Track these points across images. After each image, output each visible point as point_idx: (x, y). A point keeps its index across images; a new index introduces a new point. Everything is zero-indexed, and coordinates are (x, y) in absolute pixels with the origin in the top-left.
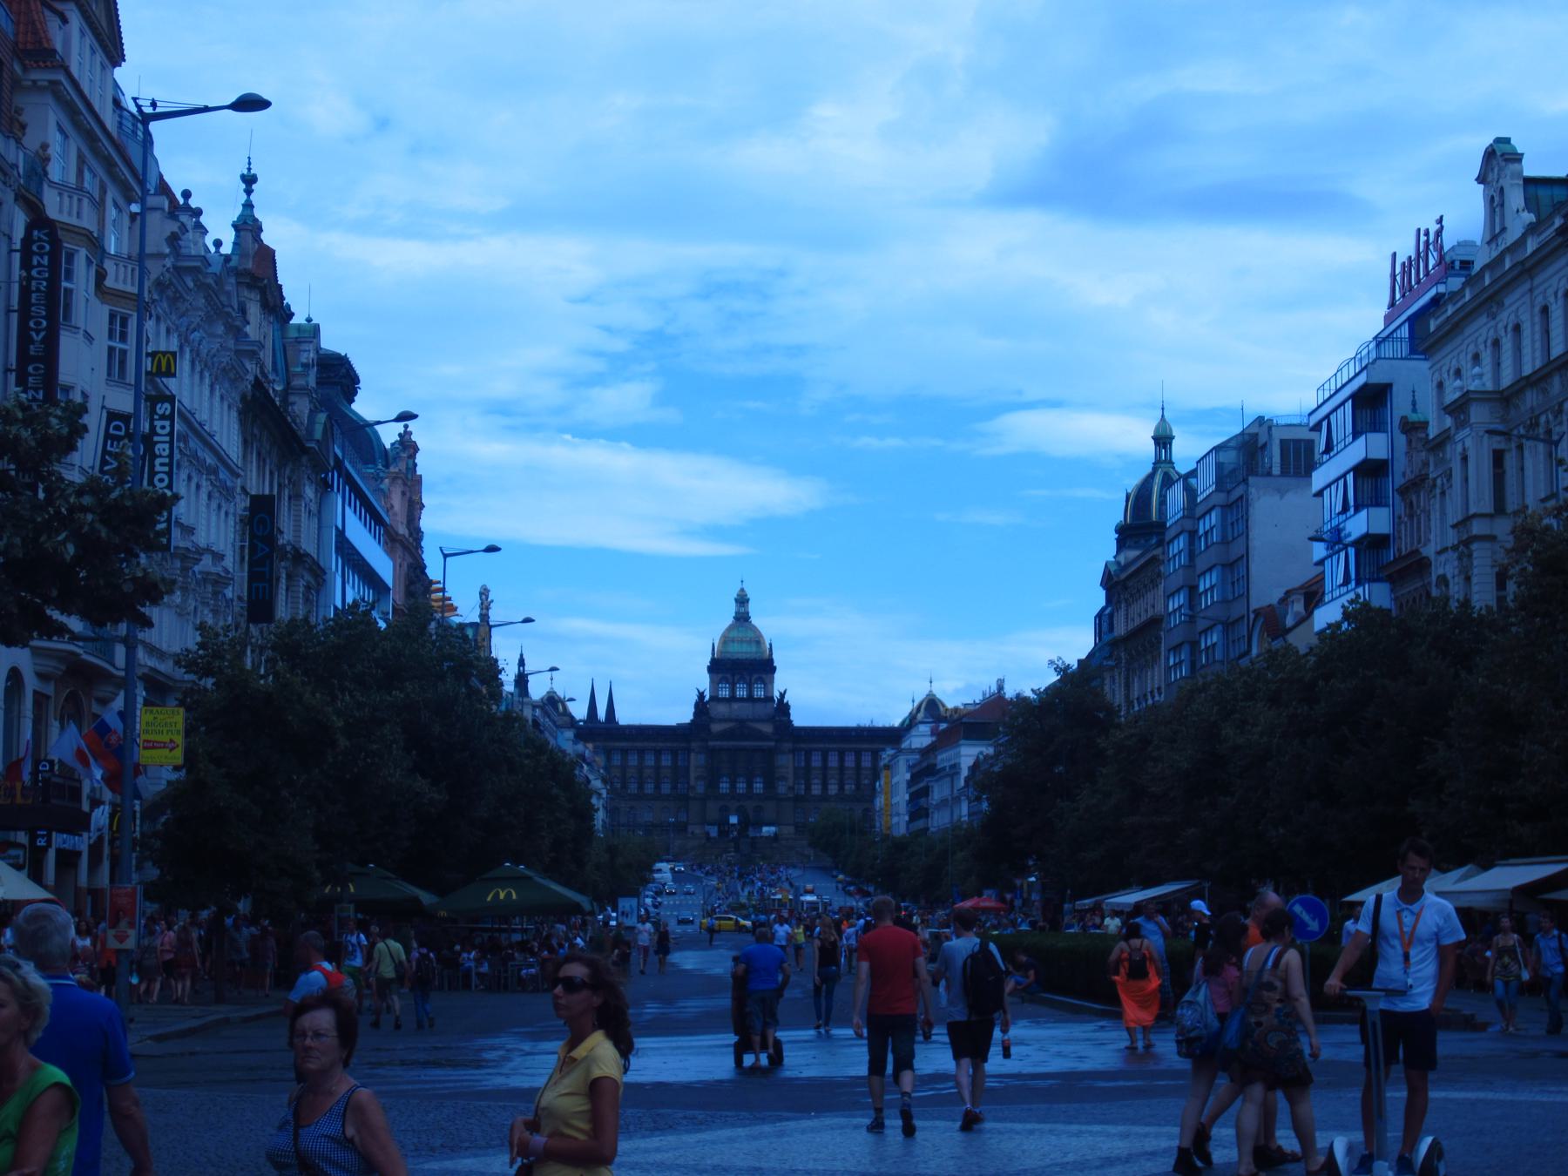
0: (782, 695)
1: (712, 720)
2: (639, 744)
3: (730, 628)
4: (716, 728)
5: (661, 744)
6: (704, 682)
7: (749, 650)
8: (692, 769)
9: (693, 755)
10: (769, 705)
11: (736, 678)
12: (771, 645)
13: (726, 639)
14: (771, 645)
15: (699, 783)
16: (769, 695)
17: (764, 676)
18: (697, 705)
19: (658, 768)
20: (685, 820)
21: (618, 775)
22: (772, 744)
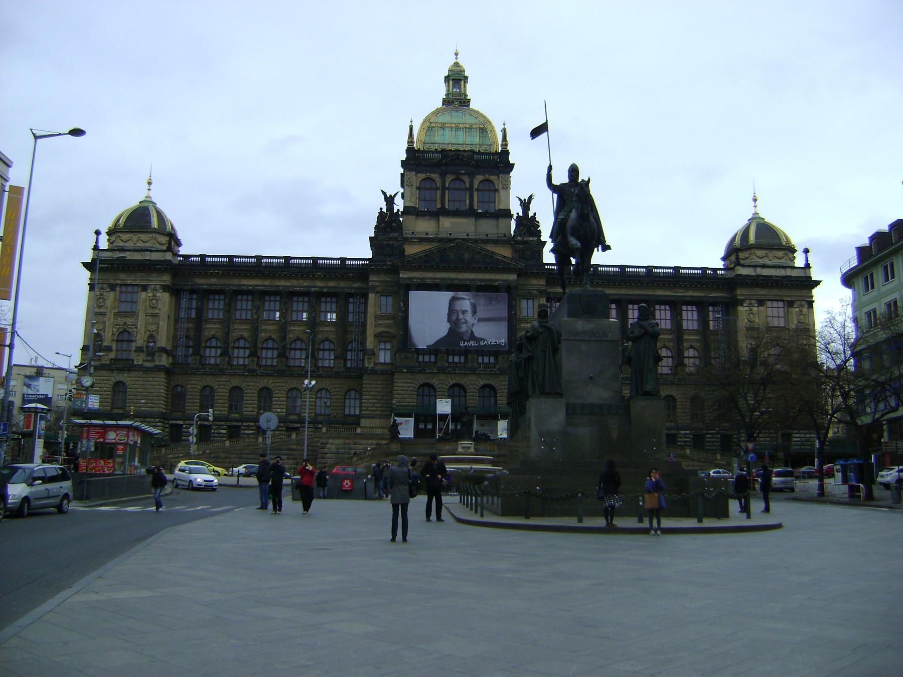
0: (526, 205)
1: (406, 240)
2: (282, 283)
3: (437, 112)
4: (411, 250)
5: (320, 284)
6: (394, 187)
7: (468, 140)
8: (370, 321)
9: (371, 296)
10: (502, 221)
11: (449, 178)
12: (504, 131)
13: (430, 125)
14: (504, 131)
15: (382, 346)
16: (502, 207)
17: (493, 178)
18: (381, 215)
19: (313, 323)
20: (357, 412)
21: (246, 334)
22: (513, 277)
